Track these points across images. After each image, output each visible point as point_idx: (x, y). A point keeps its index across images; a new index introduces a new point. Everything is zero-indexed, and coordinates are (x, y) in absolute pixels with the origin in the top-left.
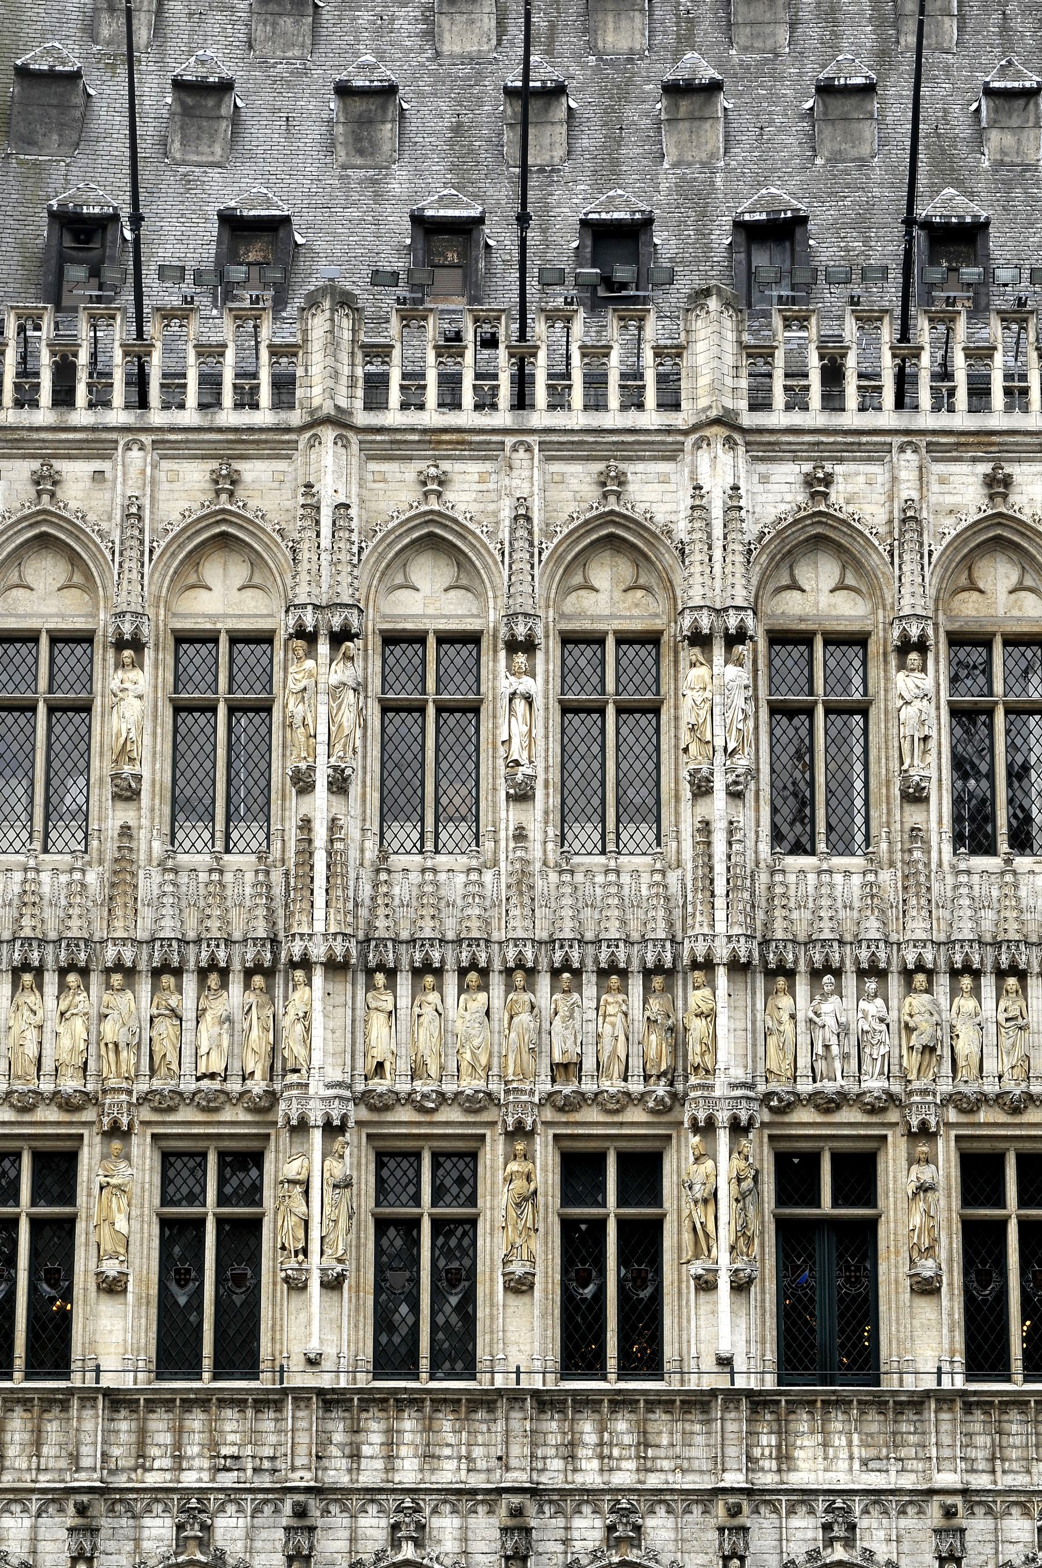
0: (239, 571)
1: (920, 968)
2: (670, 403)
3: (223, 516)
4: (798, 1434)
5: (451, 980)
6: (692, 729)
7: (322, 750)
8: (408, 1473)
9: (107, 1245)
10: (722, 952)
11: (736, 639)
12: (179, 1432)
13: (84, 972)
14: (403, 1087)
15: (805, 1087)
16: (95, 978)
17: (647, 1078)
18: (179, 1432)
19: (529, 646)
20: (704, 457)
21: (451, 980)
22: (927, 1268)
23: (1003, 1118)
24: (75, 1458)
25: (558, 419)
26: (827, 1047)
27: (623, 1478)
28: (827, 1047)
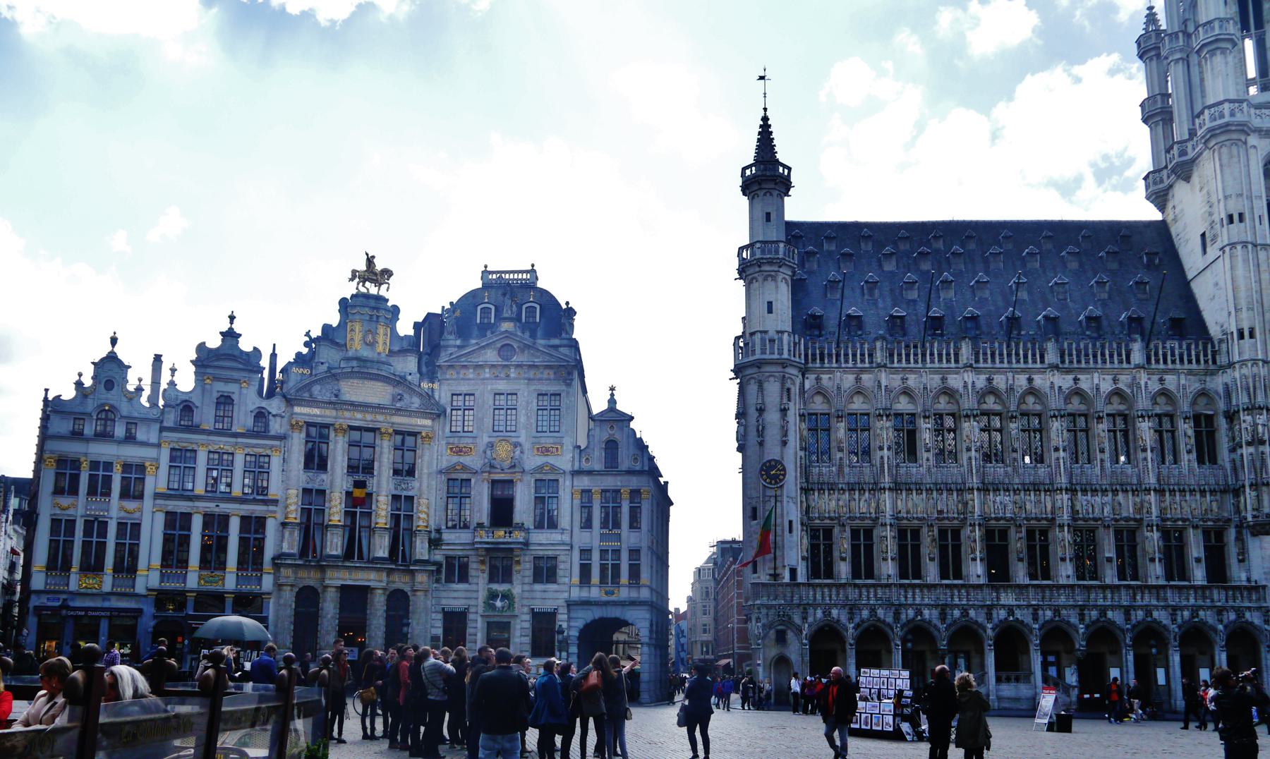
0: (861, 399)
1: (1018, 489)
2: (957, 361)
3: (859, 387)
5: (914, 492)
7: (885, 441)
8: (918, 600)
9: (842, 550)
10: (976, 486)
11: (975, 416)
12: (868, 592)
13: (834, 490)
14: (905, 516)
15: (993, 516)
16: (836, 492)
17: (958, 514)
18: (868, 592)
19: (928, 417)
20: (966, 375)
21: (914, 492)
22: (1021, 555)
24: (847, 597)
25: (932, 365)
27: (964, 602)
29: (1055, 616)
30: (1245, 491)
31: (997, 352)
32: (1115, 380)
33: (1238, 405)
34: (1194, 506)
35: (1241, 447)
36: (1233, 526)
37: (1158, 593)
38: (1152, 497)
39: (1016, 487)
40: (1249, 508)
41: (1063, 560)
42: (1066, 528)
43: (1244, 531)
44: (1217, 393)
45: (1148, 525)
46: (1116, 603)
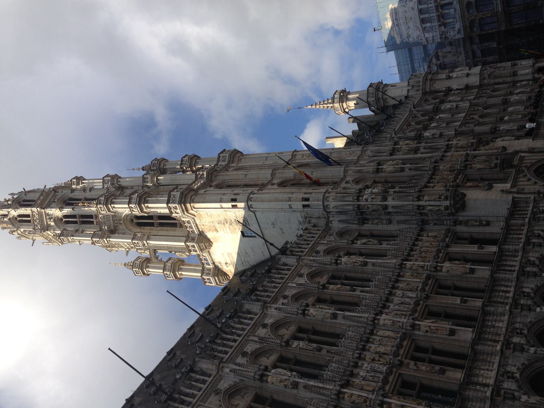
4: (478, 380)
6: (281, 381)
10: (338, 388)
23: (403, 349)
26: (371, 376)
28: (371, 376)
29: (521, 333)
30: (423, 206)
31: (225, 342)
32: (301, 276)
33: (354, 205)
34: (427, 244)
35: (386, 207)
36: (454, 228)
37: (508, 256)
38: (408, 264)
39: (356, 355)
40: (437, 203)
41: (452, 333)
42: (417, 322)
43: (461, 218)
44: (346, 227)
45: (435, 268)
46: (514, 284)
